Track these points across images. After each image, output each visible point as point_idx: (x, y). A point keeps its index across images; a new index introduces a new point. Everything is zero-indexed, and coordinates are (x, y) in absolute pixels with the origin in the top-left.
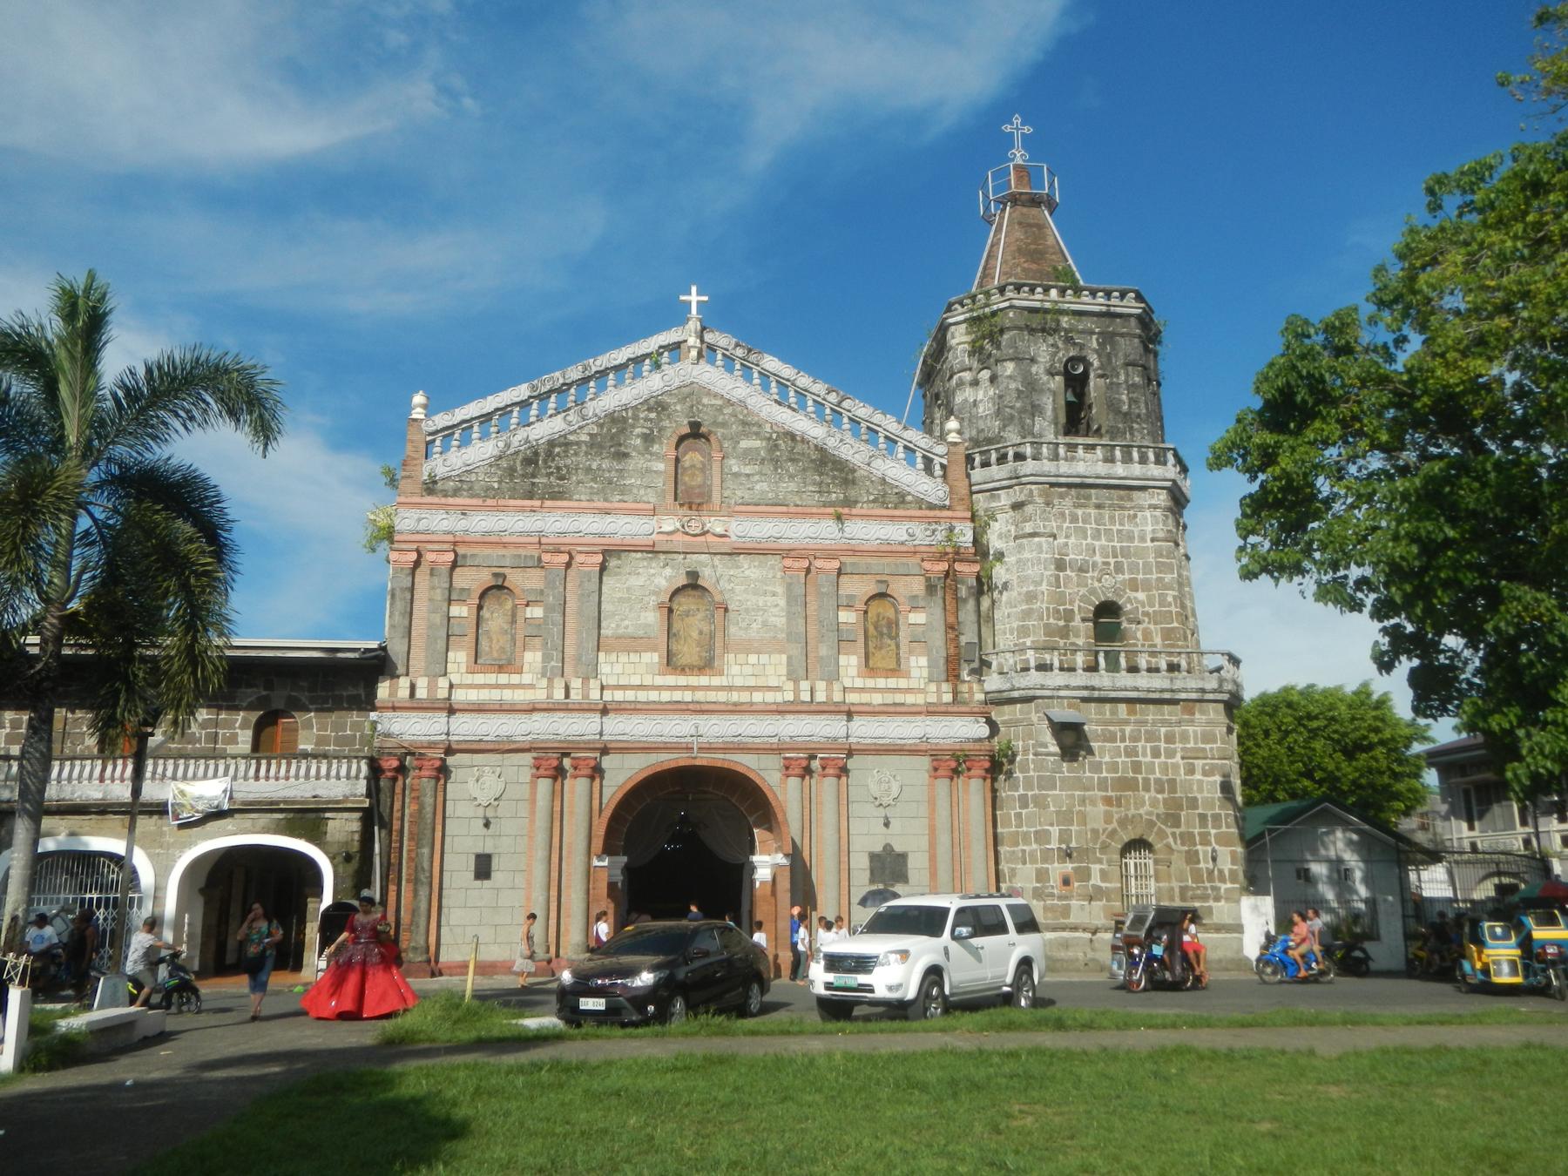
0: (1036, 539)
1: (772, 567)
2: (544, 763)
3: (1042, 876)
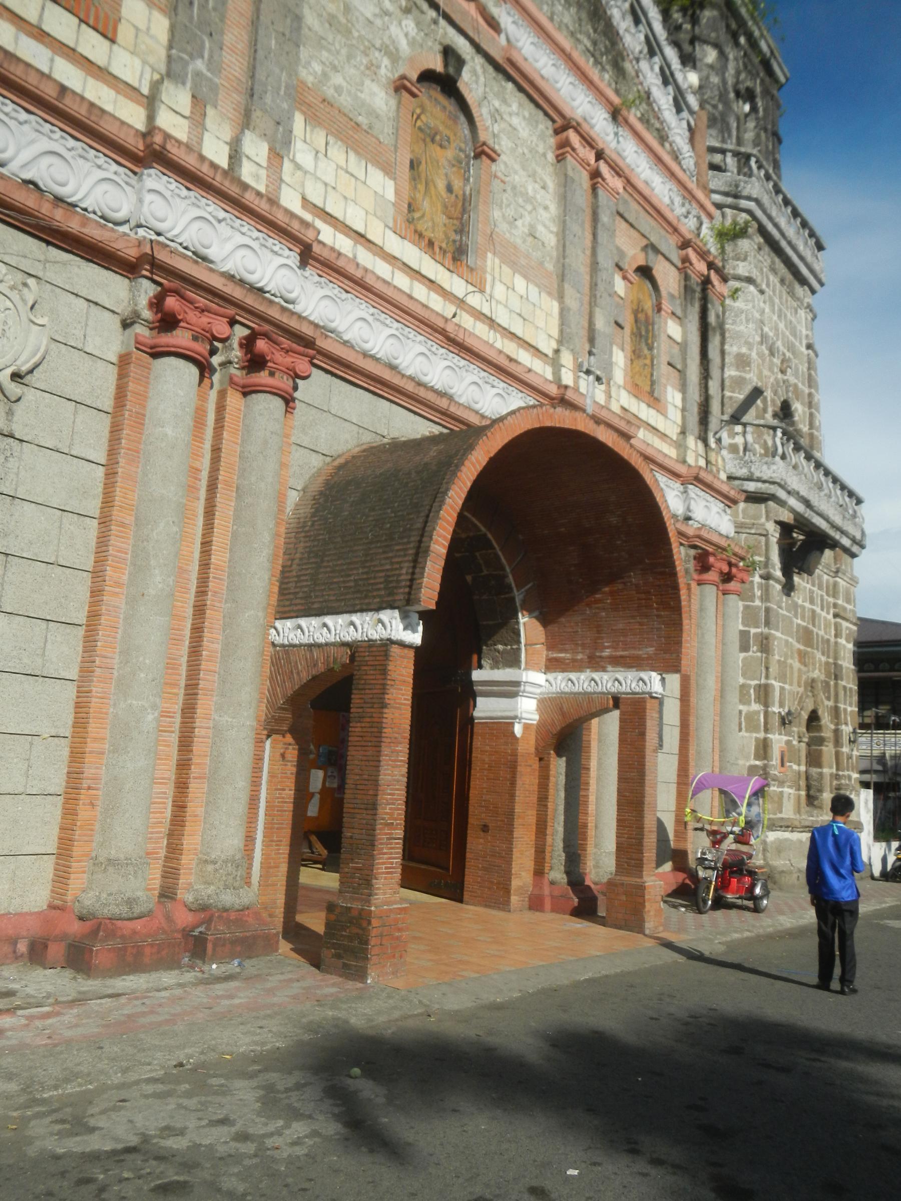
0: (752, 288)
1: (542, 137)
2: (192, 316)
3: (763, 748)
